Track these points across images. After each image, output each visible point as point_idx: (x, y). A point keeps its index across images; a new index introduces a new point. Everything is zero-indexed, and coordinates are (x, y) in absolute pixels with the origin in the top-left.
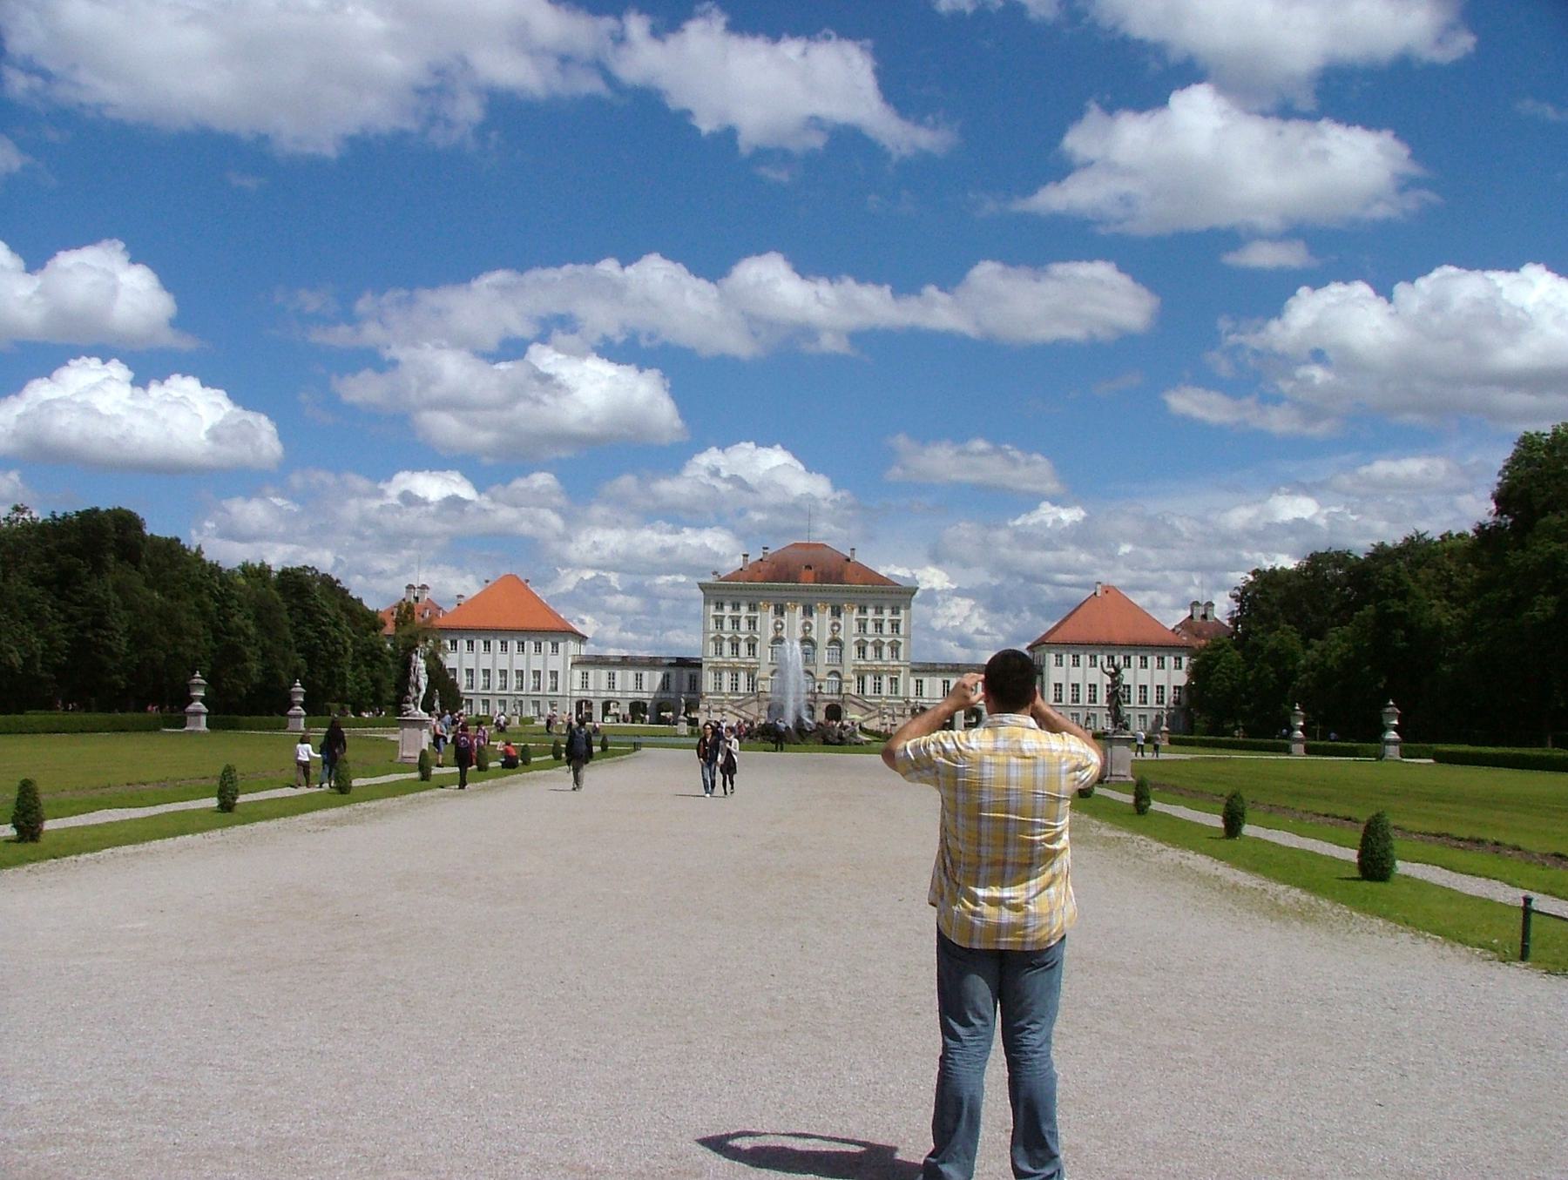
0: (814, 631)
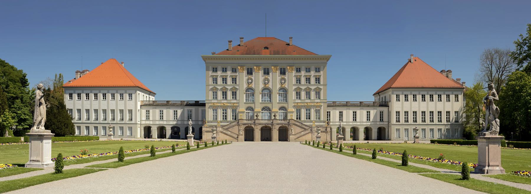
0: (270, 83)
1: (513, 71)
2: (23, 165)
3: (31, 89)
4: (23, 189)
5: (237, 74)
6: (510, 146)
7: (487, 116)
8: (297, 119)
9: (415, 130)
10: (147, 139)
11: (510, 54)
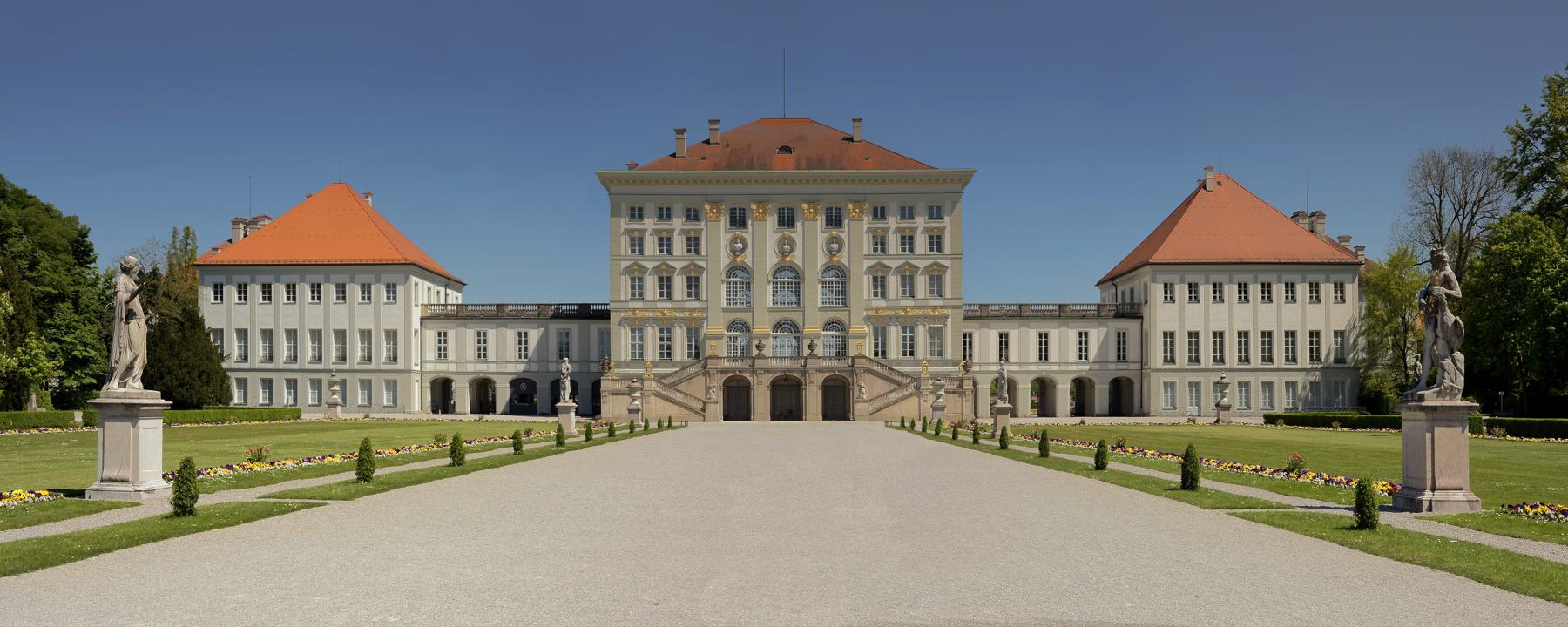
0: (798, 252)
1: (1504, 212)
2: (81, 493)
3: (101, 272)
4: (79, 563)
5: (702, 225)
6: (1497, 430)
7: (1427, 345)
8: (876, 354)
9: (1220, 386)
10: (440, 416)
11: (1495, 163)
